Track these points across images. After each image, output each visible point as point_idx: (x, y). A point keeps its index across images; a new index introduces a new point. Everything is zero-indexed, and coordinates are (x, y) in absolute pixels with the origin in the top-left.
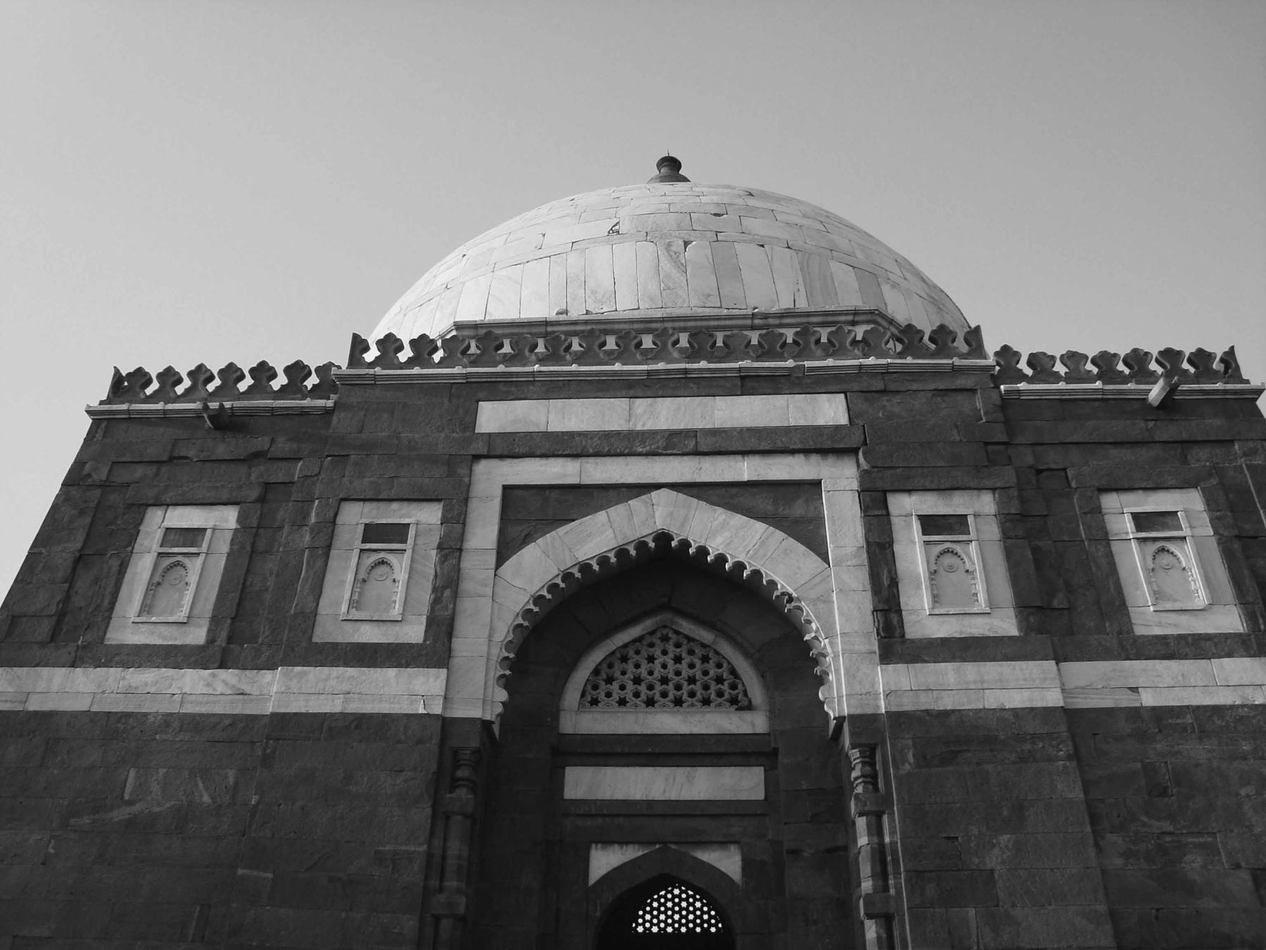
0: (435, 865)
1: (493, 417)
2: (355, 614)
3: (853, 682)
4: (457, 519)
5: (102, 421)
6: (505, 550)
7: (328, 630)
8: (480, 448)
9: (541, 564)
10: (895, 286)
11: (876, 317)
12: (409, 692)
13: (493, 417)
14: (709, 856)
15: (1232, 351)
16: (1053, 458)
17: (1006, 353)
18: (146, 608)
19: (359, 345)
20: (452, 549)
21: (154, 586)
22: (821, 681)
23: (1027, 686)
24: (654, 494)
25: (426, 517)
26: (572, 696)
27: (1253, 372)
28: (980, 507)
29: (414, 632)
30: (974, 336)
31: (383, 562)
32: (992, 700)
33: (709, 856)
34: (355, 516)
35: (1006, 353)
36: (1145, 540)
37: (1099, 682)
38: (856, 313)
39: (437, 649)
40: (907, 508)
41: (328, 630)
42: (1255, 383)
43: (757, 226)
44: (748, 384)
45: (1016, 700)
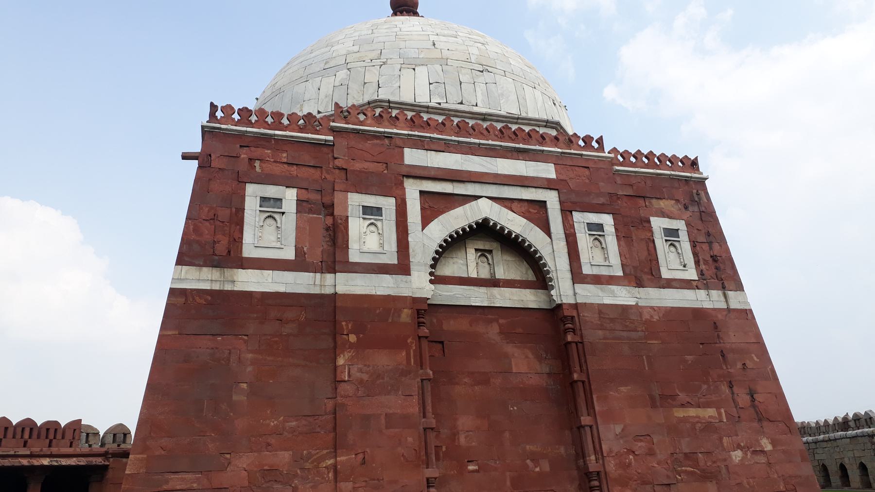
2: (365, 249)
3: (565, 291)
8: (404, 171)
11: (557, 125)
15: (696, 158)
17: (614, 150)
22: (552, 287)
24: (480, 200)
25: (388, 204)
27: (704, 169)
28: (607, 220)
30: (600, 141)
31: (372, 224)
35: (614, 150)
36: (666, 240)
38: (547, 121)
41: (354, 257)
42: (705, 175)
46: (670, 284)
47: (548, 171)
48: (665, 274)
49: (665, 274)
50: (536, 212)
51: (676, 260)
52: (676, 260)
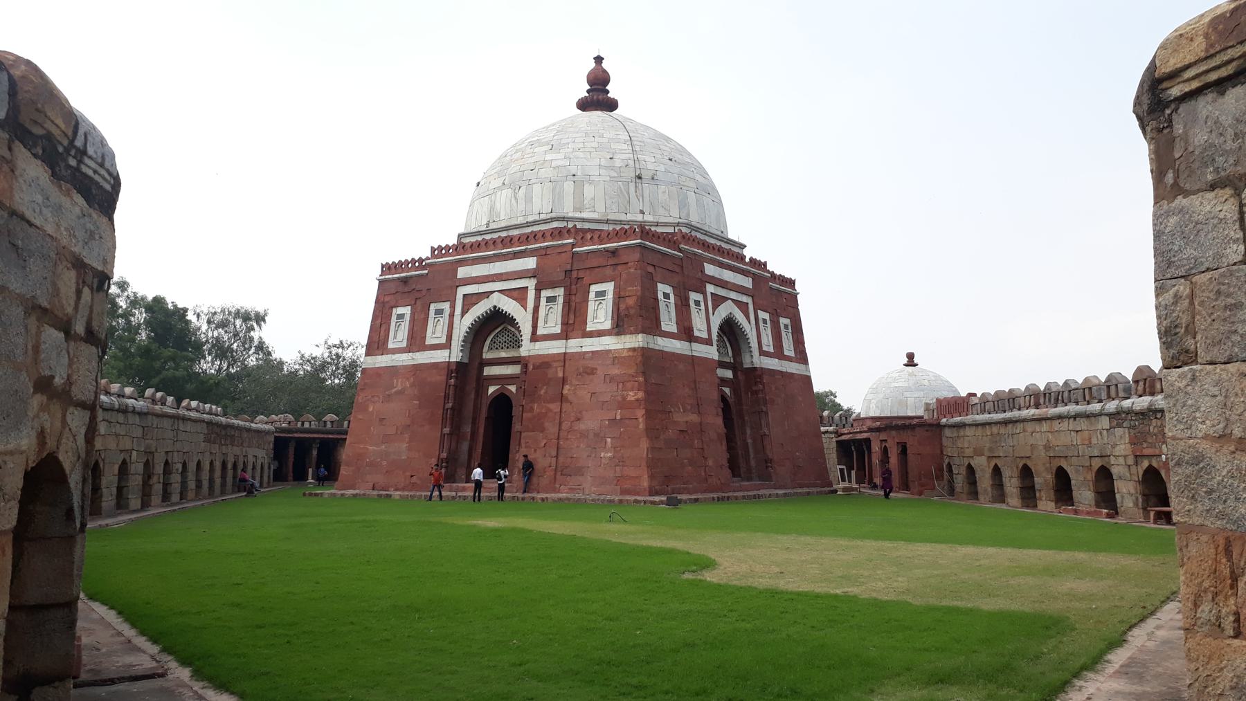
0: (446, 397)
1: (462, 272)
3: (528, 348)
4: (453, 307)
5: (381, 282)
6: (464, 313)
7: (429, 341)
9: (469, 319)
10: (591, 182)
12: (440, 356)
13: (462, 272)
14: (510, 387)
16: (581, 274)
18: (395, 337)
19: (433, 250)
20: (452, 315)
21: (396, 331)
23: (556, 347)
25: (446, 306)
26: (486, 348)
28: (560, 292)
29: (443, 340)
32: (550, 352)
33: (510, 387)
34: (433, 307)
37: (575, 345)
39: (447, 345)
40: (545, 294)
41: (429, 341)
43: (545, 173)
44: (516, 256)
45: (555, 351)
46: (592, 335)
47: (530, 263)
48: (590, 327)
49: (590, 327)
50: (519, 295)
51: (600, 314)
52: (600, 314)
